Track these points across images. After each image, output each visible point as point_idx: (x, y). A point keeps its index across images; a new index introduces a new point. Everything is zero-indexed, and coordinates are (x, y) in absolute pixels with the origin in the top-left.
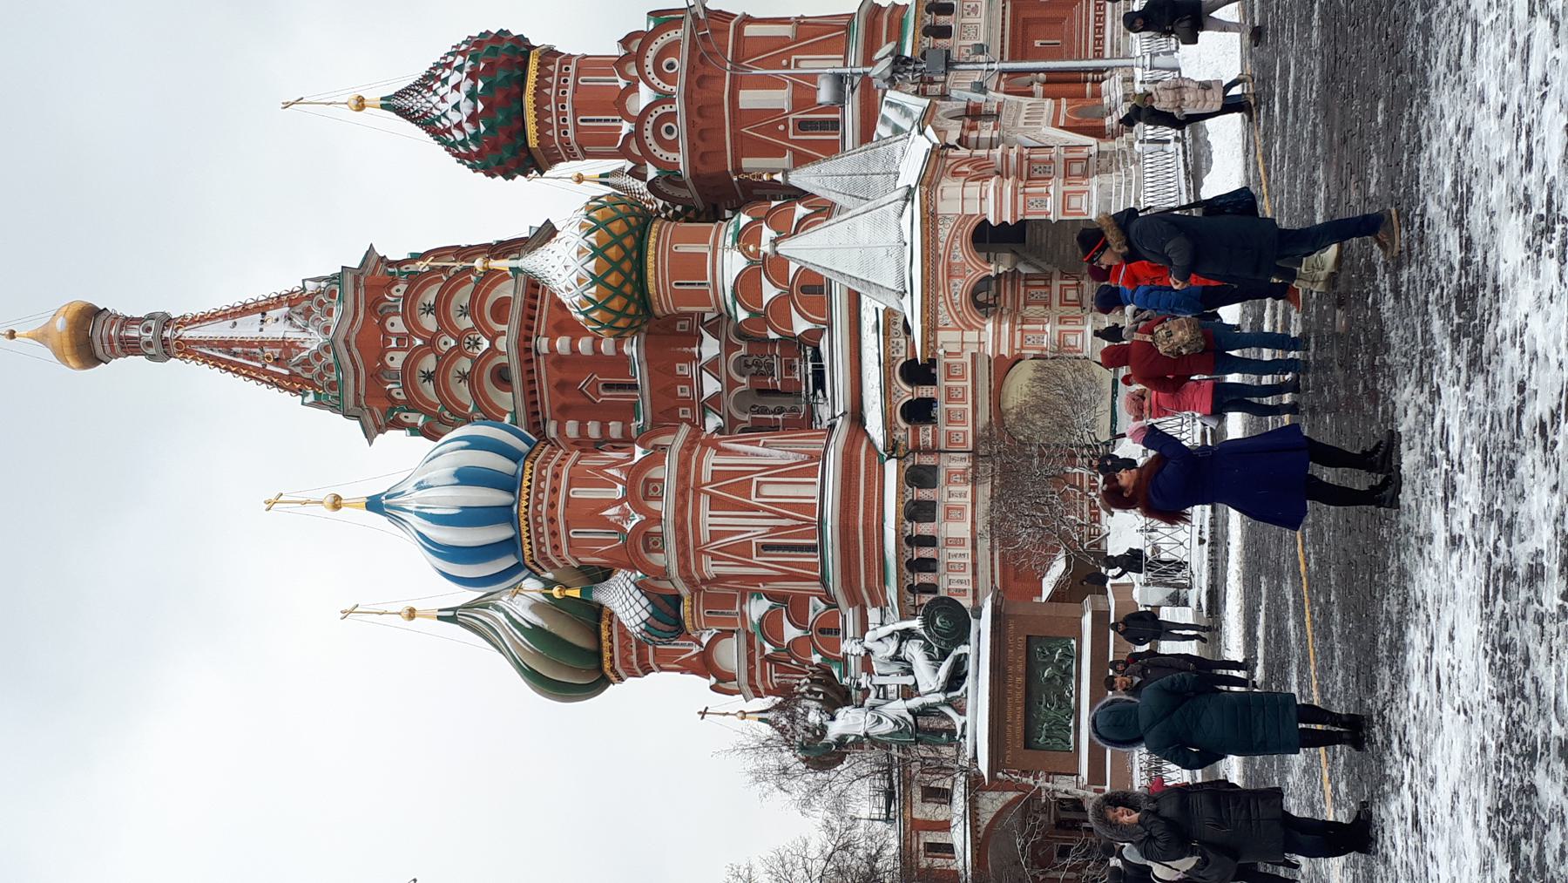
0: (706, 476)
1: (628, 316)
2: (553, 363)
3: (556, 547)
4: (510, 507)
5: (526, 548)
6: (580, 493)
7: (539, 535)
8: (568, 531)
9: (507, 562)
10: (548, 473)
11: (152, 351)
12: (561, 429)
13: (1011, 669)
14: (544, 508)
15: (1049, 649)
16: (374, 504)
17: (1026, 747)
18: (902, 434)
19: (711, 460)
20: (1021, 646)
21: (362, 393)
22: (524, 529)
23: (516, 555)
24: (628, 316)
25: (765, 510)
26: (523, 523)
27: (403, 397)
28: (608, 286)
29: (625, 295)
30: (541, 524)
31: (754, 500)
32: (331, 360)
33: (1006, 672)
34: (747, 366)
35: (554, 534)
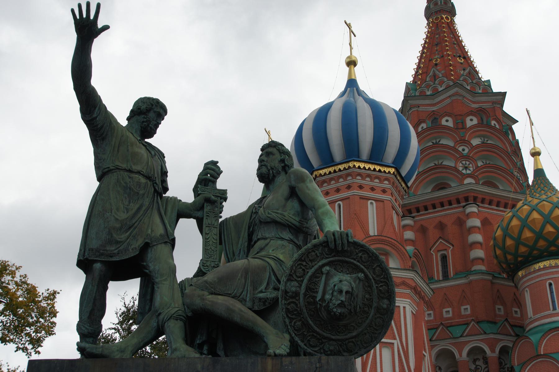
1: (517, 248)
2: (459, 218)
4: (359, 157)
5: (326, 171)
6: (372, 210)
7: (337, 179)
8: (342, 200)
9: (314, 159)
10: (386, 185)
11: (432, 6)
14: (359, 180)
16: (352, 83)
21: (421, 109)
22: (341, 167)
23: (320, 166)
24: (517, 248)
26: (346, 166)
27: (420, 129)
28: (543, 227)
29: (536, 242)
30: (345, 180)
32: (440, 89)
34: (475, 361)
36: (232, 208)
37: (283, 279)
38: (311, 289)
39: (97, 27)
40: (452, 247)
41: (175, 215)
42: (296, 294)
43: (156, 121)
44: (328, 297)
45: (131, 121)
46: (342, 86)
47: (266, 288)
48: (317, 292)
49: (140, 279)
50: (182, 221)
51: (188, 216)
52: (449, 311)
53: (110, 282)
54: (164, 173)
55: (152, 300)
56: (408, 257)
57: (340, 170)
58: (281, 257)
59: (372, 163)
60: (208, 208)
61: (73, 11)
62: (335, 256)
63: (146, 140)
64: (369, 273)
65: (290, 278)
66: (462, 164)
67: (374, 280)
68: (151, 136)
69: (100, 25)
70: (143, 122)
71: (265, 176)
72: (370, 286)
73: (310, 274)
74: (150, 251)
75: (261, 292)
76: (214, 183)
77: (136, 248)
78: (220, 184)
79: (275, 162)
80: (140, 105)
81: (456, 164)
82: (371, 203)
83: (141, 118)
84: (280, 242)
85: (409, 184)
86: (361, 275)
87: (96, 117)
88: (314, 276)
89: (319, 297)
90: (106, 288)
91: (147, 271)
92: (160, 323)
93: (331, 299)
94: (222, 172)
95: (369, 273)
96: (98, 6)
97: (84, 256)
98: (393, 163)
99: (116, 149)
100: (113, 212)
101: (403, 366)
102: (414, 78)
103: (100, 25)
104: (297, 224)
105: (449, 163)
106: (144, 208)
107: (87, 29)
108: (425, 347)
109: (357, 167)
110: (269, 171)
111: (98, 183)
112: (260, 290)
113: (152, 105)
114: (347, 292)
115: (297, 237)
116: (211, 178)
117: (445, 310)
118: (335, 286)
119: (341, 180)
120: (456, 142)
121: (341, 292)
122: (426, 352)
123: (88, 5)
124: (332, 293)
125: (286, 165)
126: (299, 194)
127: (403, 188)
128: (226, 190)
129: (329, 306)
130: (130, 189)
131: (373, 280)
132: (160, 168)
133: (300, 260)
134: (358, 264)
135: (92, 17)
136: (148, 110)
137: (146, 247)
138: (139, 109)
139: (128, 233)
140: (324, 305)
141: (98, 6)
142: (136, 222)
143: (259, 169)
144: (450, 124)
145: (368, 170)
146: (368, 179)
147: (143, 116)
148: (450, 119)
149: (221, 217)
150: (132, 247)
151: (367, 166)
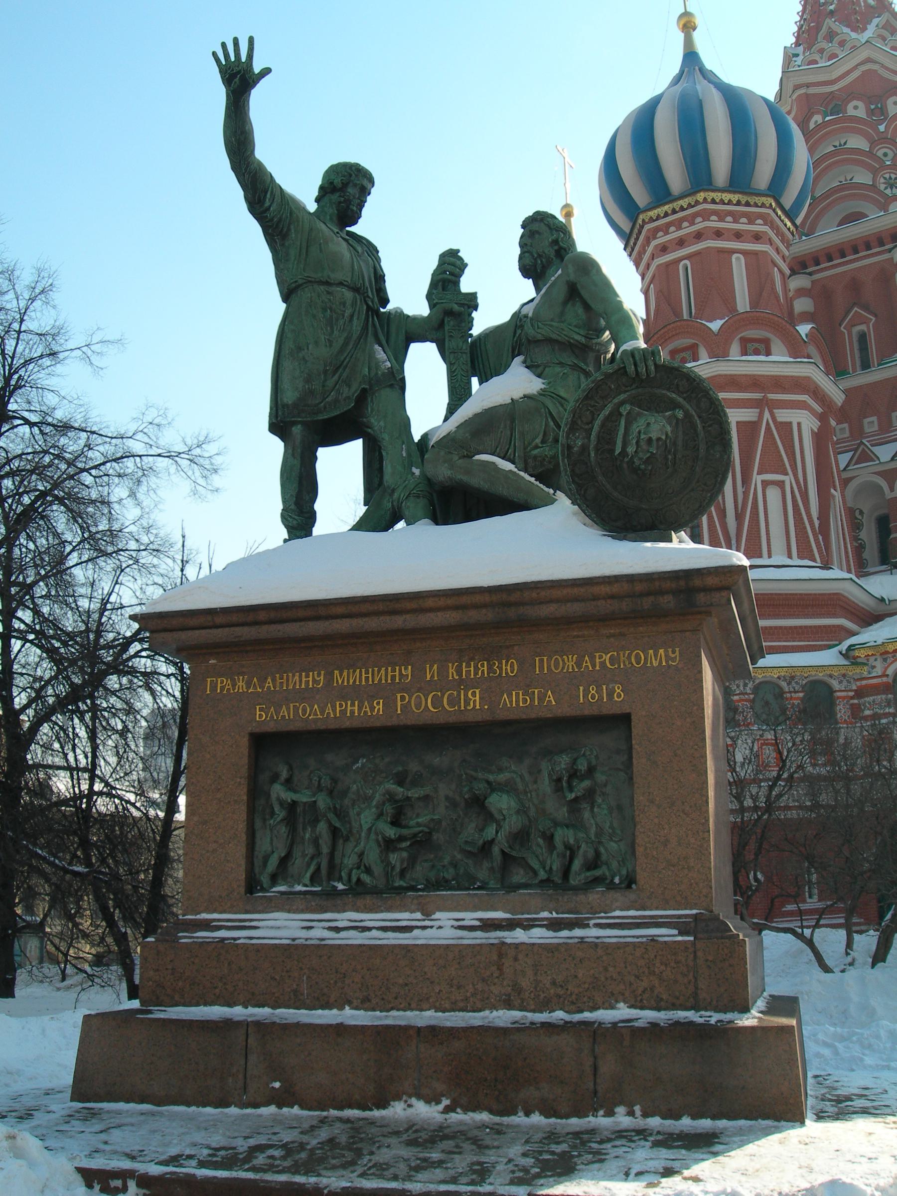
0: (783, 415)
3: (664, 249)
4: (711, 184)
5: (660, 211)
6: (739, 267)
7: (678, 224)
9: (640, 196)
10: (759, 227)
12: (801, 292)
13: (508, 668)
14: (714, 223)
15: (590, 795)
17: (263, 743)
18: (878, 671)
19: (805, 422)
20: (591, 698)
21: (812, 90)
22: (684, 203)
25: (746, 494)
27: (812, 126)
30: (692, 223)
31: (757, 479)
33: (492, 654)
35: (681, 243)
36: (483, 321)
37: (564, 428)
38: (607, 438)
39: (253, 73)
40: (874, 319)
41: (402, 337)
42: (584, 448)
43: (359, 198)
44: (631, 450)
45: (322, 203)
46: (674, 64)
47: (543, 442)
48: (615, 443)
49: (361, 440)
50: (414, 348)
51: (422, 339)
52: (873, 422)
53: (320, 449)
54: (379, 278)
55: (381, 470)
56: (802, 343)
57: (682, 209)
58: (562, 394)
59: (734, 192)
60: (450, 323)
61: (214, 54)
62: (637, 387)
63: (348, 229)
64: (690, 409)
65: (573, 427)
66: (885, 178)
67: (700, 417)
68: (355, 222)
69: (257, 69)
70: (340, 202)
71: (532, 266)
72: (693, 426)
73: (601, 417)
74: (369, 399)
75: (537, 447)
76: (457, 283)
77: (348, 398)
78: (466, 285)
79: (544, 245)
80: (333, 177)
81: (874, 180)
82: (738, 259)
83: (335, 197)
84: (558, 369)
85: (798, 221)
86: (680, 414)
87: (270, 206)
88: (607, 419)
89: (618, 450)
90: (315, 458)
91: (370, 430)
92: (395, 504)
93: (636, 452)
94: (466, 265)
95: (690, 409)
96: (251, 40)
97: (277, 416)
98: (769, 188)
99: (304, 251)
100: (310, 347)
101: (800, 514)
102: (798, 38)
103: (257, 69)
104: (583, 340)
105: (863, 177)
106: (355, 337)
107: (239, 79)
108: (834, 482)
109: (709, 200)
110: (535, 260)
111: (284, 305)
112: (534, 444)
113: (351, 175)
114: (659, 439)
115: (585, 361)
116: (450, 277)
117: (866, 421)
118: (639, 432)
119: (685, 224)
120: (873, 143)
121: (650, 440)
122: (835, 490)
123: (236, 42)
124: (637, 442)
125: (561, 248)
126: (583, 292)
127: (789, 229)
128: (476, 293)
129: (634, 462)
130: (331, 309)
131: (696, 418)
132: (372, 270)
133: (587, 397)
134: (674, 396)
135: (244, 59)
136: (345, 185)
137: (363, 398)
138: (332, 183)
139: (336, 377)
140: (626, 460)
141: (251, 40)
142: (345, 359)
143: (521, 258)
144: (861, 113)
145: (728, 204)
146: (729, 219)
147: (338, 194)
148: (860, 104)
149: (471, 336)
150: (344, 395)
151: (726, 197)
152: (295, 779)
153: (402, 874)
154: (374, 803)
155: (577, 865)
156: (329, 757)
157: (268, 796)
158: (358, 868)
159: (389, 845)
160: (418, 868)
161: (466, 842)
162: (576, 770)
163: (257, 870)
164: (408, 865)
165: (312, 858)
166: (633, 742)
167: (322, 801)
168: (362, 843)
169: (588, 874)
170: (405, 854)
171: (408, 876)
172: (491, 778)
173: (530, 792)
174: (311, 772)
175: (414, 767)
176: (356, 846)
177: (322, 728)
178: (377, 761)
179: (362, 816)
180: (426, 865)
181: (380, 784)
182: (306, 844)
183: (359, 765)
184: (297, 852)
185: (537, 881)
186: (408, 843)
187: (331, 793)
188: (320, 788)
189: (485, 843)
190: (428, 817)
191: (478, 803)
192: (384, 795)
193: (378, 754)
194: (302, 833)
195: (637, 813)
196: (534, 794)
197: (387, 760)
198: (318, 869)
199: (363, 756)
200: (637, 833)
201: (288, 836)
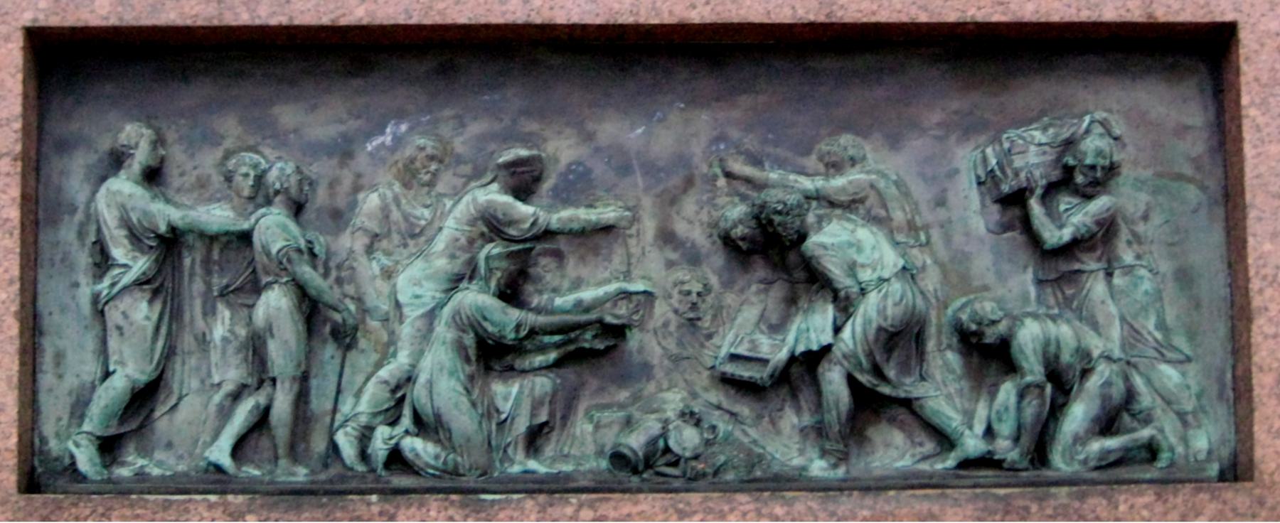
152: (172, 172)
153: (535, 438)
154: (440, 243)
155: (1078, 414)
156: (288, 115)
157: (91, 217)
158: (393, 423)
159: (490, 355)
160: (582, 426)
161: (734, 358)
162: (1069, 171)
163: (48, 428)
164: (552, 414)
165: (236, 396)
166: (1245, 100)
167: (273, 229)
168: (404, 357)
169: (1112, 443)
170: (543, 384)
171: (549, 450)
172: (808, 184)
173: (926, 228)
174: (228, 155)
175: (562, 149)
176: (379, 365)
177: (274, 22)
178: (446, 130)
179: (402, 280)
180: (607, 416)
181: (457, 194)
182: (215, 357)
183: (388, 139)
184: (184, 376)
185: (951, 462)
186: (552, 356)
187: (298, 209)
188: (261, 194)
189: (793, 359)
190: (613, 287)
191: (773, 250)
192: (472, 222)
193: (448, 112)
194: (200, 323)
195: (1255, 285)
196: (936, 235)
197: (476, 128)
198: (262, 421)
199: (400, 115)
200: (1256, 338)
201: (157, 329)
